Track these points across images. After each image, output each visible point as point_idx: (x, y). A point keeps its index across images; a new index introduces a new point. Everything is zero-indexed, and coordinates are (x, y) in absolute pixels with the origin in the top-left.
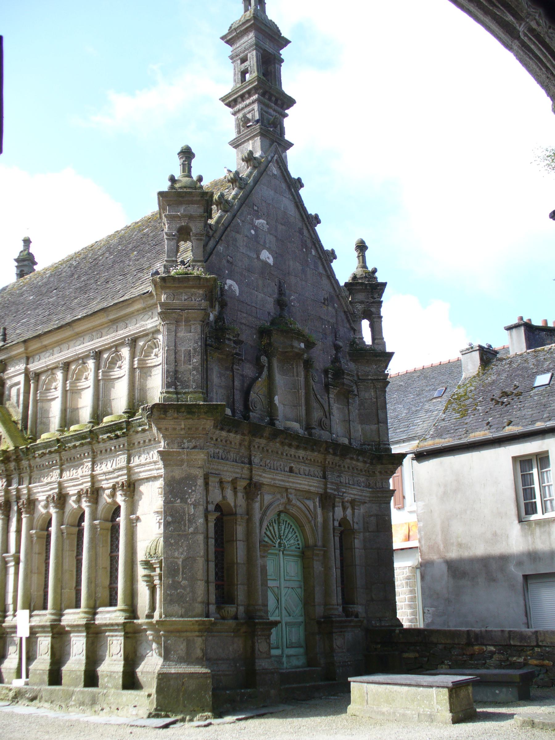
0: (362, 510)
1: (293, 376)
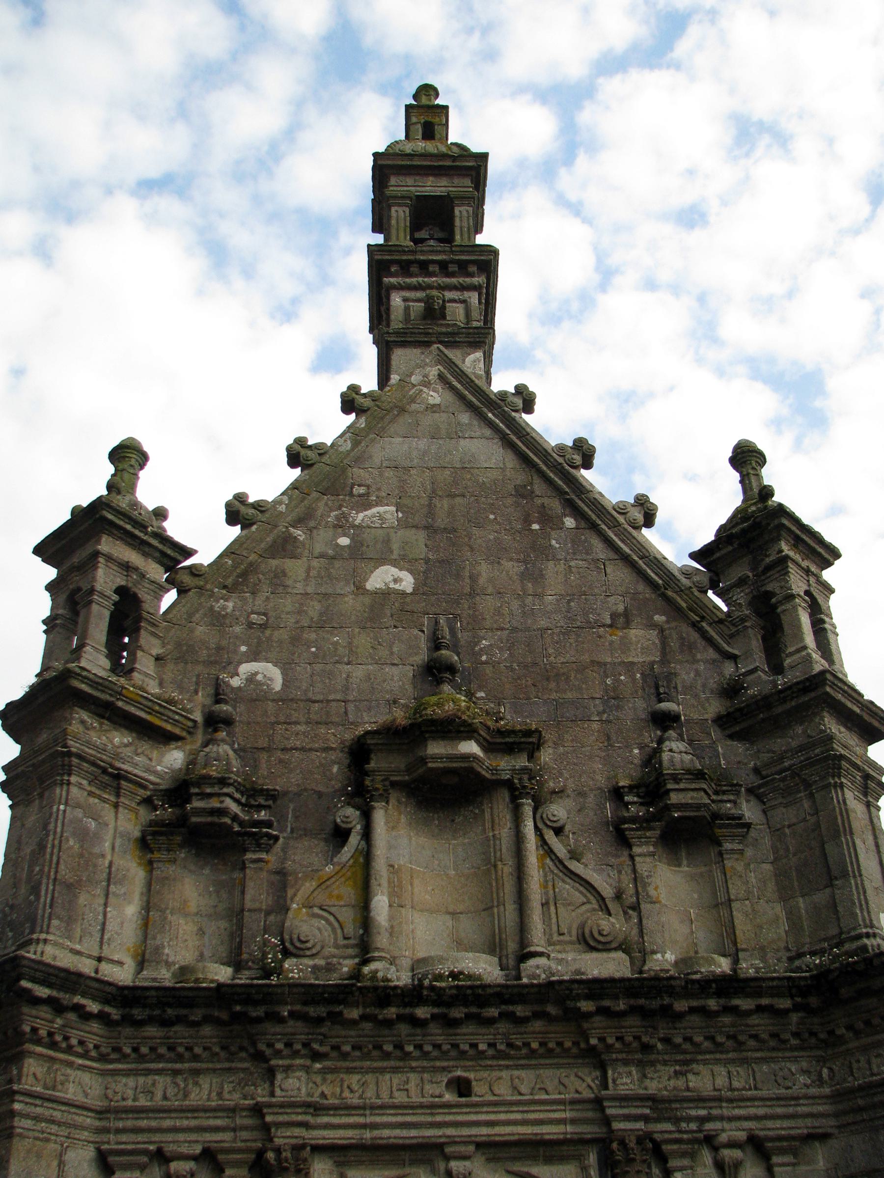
1: (484, 830)
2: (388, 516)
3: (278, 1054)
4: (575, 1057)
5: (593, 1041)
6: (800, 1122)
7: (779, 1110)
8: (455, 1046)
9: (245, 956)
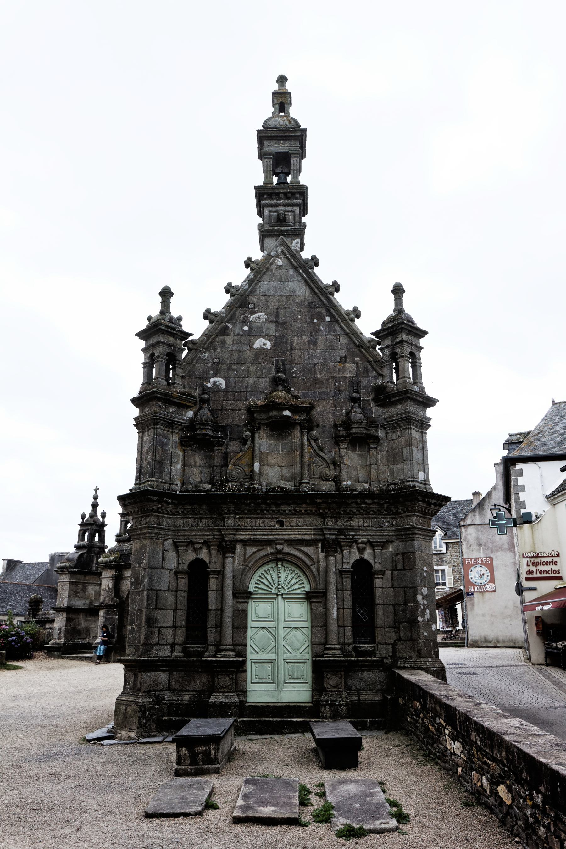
0: (391, 549)
2: (262, 317)
3: (226, 513)
4: (316, 515)
5: (321, 511)
6: (384, 537)
7: (378, 534)
8: (279, 511)
9: (215, 481)
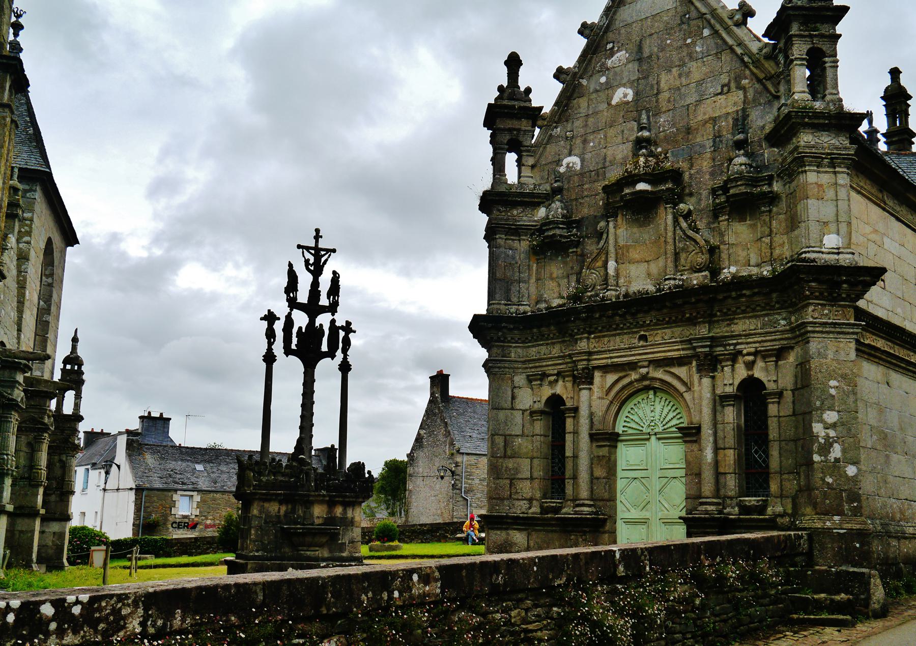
2: (622, 58)
3: (577, 334)
